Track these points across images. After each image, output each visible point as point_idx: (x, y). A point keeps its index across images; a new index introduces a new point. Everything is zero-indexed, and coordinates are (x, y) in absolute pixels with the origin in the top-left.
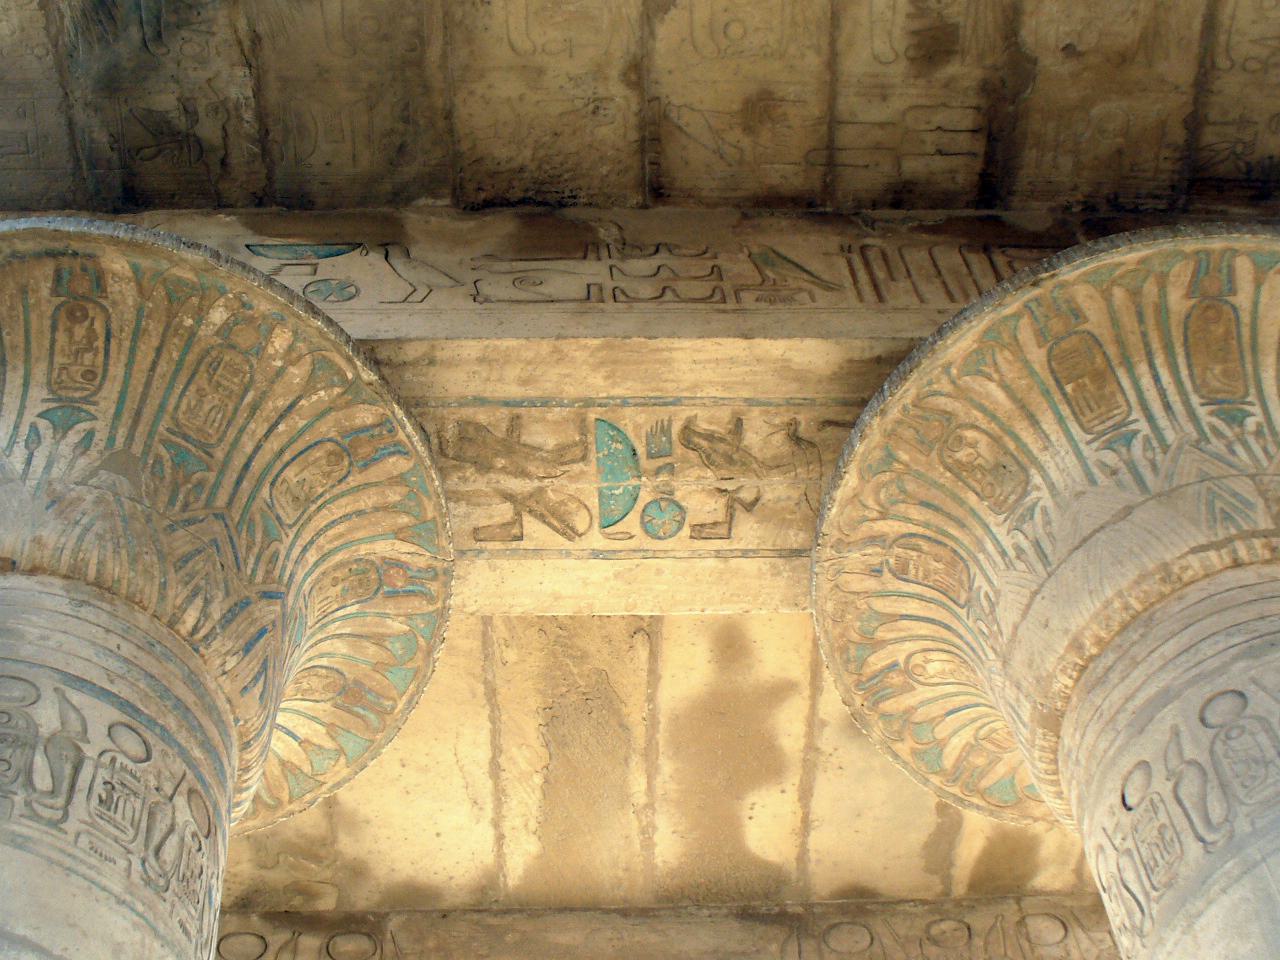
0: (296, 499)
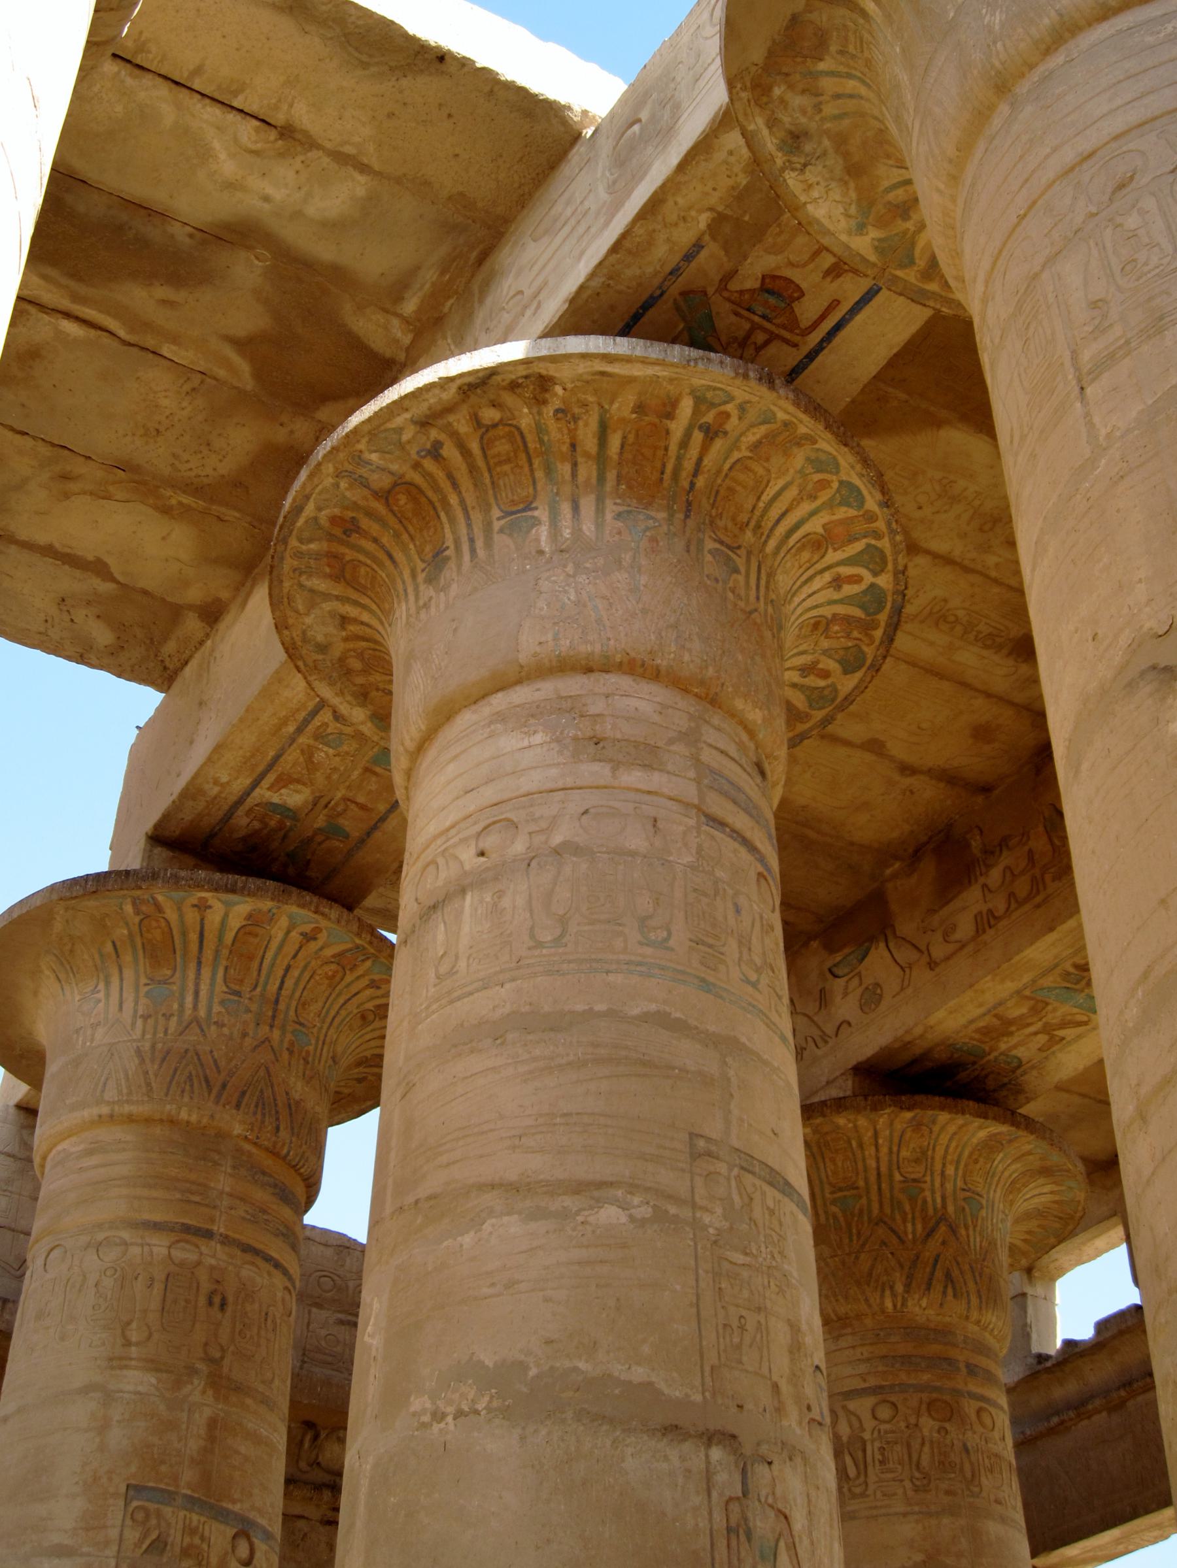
0: (917, 1161)
